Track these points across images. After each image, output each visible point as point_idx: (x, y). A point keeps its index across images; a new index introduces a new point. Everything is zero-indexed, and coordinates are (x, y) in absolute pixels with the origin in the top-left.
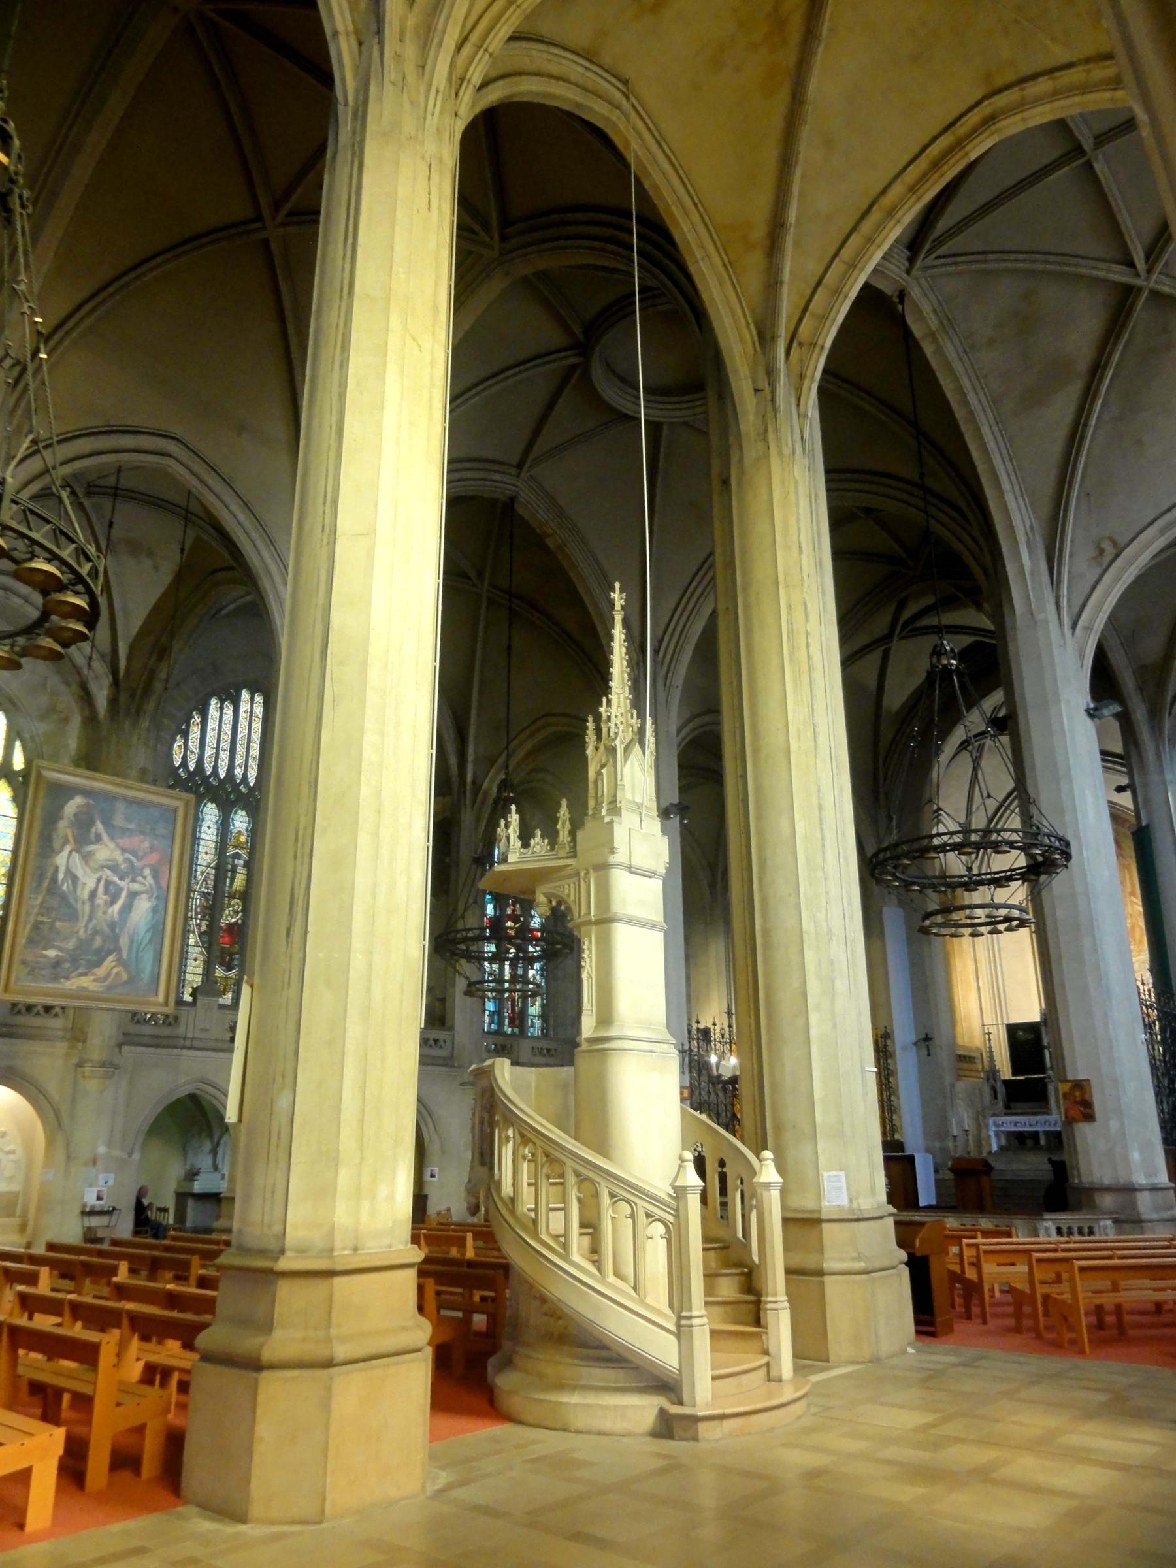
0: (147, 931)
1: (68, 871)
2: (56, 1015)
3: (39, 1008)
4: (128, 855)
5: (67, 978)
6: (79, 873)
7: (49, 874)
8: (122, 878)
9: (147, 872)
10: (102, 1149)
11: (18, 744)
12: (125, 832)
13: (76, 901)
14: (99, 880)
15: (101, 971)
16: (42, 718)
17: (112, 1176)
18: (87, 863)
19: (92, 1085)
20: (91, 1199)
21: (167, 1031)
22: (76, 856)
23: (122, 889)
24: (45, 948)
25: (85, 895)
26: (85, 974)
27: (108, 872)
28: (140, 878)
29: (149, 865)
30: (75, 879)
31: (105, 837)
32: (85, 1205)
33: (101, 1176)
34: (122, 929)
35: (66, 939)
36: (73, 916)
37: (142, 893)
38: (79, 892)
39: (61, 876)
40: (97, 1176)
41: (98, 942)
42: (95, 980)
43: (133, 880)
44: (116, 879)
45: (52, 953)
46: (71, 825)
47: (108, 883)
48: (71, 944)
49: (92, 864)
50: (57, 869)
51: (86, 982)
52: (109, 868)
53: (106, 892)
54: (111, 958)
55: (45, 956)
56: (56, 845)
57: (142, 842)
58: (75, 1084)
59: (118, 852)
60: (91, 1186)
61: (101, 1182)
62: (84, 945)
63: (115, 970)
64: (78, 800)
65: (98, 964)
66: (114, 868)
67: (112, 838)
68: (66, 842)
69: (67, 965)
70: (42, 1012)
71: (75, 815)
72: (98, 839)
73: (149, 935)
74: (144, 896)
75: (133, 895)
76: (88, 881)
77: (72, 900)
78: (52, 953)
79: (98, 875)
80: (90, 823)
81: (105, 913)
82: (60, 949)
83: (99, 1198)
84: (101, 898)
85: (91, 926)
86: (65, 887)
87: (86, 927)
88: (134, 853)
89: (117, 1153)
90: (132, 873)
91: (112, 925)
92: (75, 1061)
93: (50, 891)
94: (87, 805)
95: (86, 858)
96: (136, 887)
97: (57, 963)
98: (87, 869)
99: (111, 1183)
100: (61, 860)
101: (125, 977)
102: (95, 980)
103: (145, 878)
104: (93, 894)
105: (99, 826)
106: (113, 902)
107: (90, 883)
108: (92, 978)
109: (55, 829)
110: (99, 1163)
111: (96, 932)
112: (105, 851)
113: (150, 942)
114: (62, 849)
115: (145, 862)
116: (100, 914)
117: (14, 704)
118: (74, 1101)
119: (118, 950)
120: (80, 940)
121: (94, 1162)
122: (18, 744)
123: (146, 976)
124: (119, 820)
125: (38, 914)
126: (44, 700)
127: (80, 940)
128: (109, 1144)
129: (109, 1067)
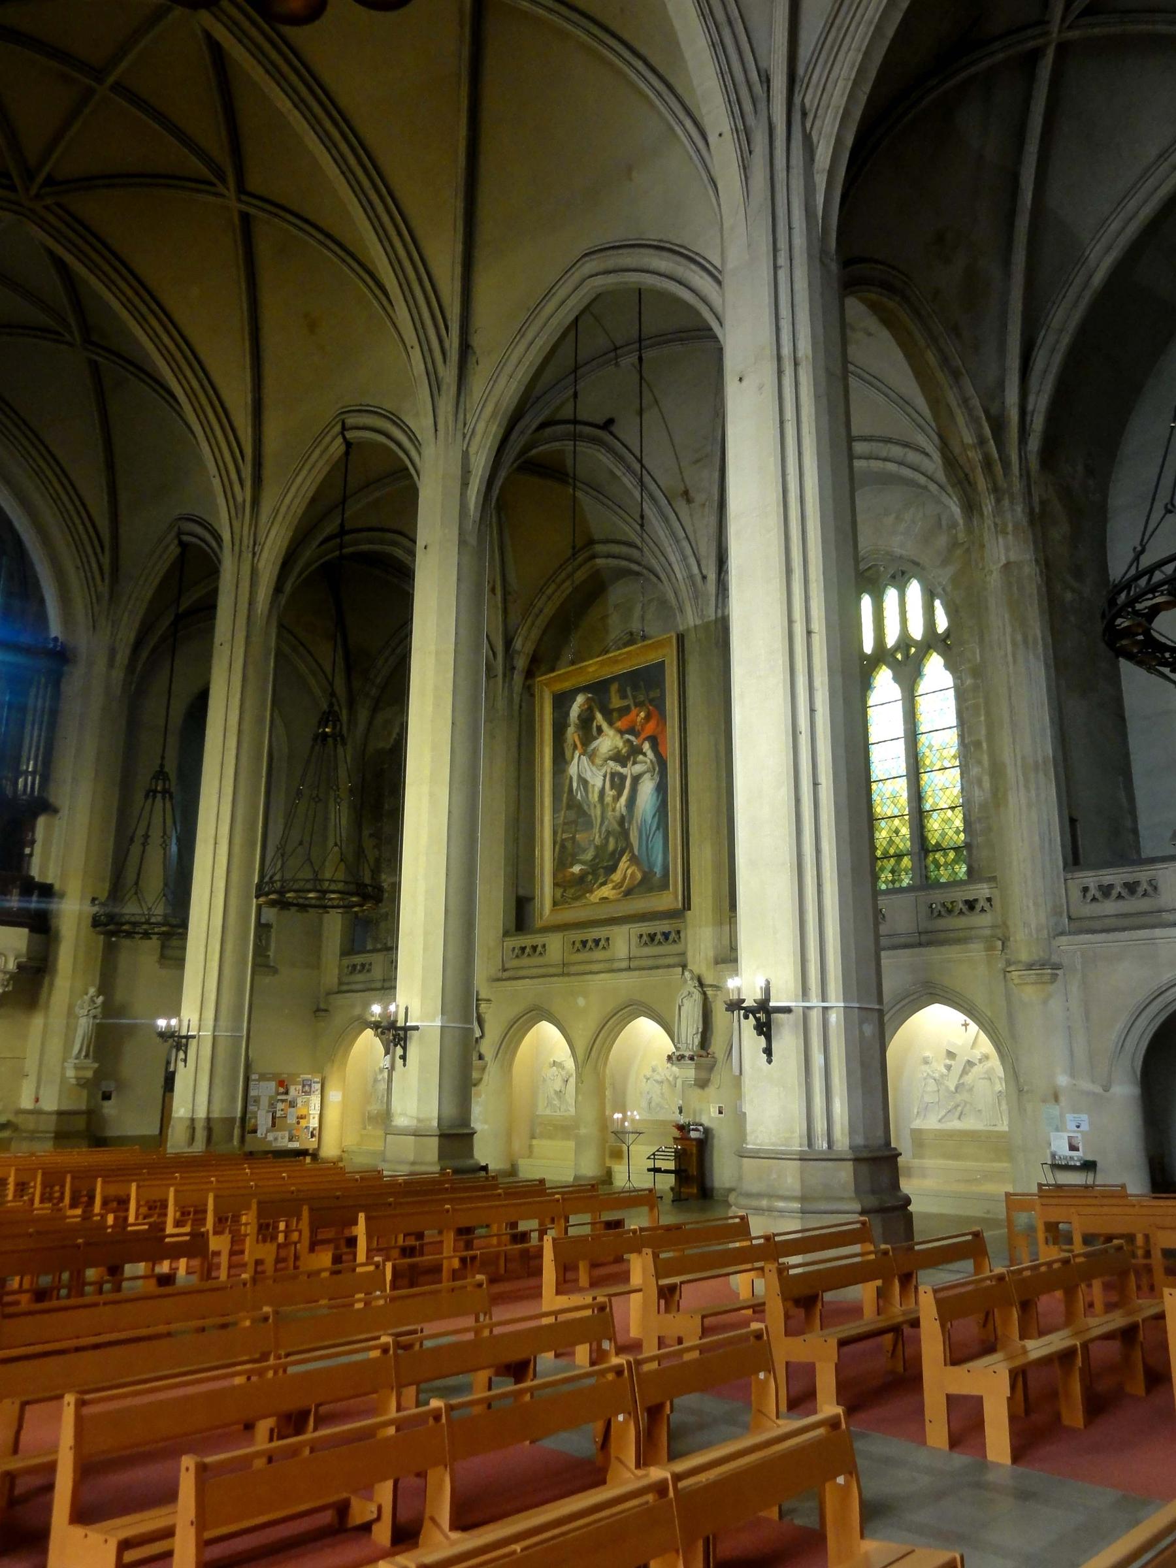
0: (654, 816)
1: (579, 776)
2: (983, 910)
3: (961, 905)
4: (627, 736)
5: (591, 892)
6: (588, 776)
7: (566, 789)
8: (624, 766)
9: (646, 747)
10: (1063, 1080)
11: (937, 603)
12: (625, 711)
14: (605, 776)
15: (617, 877)
16: (945, 562)
17: (1085, 1117)
18: (593, 763)
19: (1029, 993)
20: (1060, 1146)
21: (1143, 904)
22: (584, 758)
23: (626, 777)
24: (571, 866)
25: (594, 797)
26: (604, 884)
27: (611, 763)
28: (641, 757)
29: (646, 739)
30: (584, 782)
31: (605, 726)
32: (1053, 1156)
33: (1069, 1117)
34: (630, 823)
35: (584, 851)
36: (589, 825)
37: (645, 773)
38: (590, 795)
39: (575, 785)
40: (1062, 1116)
41: (611, 846)
42: (614, 888)
43: (635, 763)
44: (619, 769)
45: (576, 869)
46: (577, 726)
47: (613, 775)
48: (589, 855)
49: (598, 761)
50: (571, 778)
51: (606, 891)
52: (611, 759)
53: (612, 788)
54: (624, 859)
55: (573, 874)
56: (568, 754)
57: (638, 715)
58: (1008, 996)
59: (618, 737)
60: (1057, 1130)
61: (1071, 1126)
62: (600, 849)
63: (629, 871)
64: (580, 699)
65: (613, 869)
66: (619, 758)
67: (611, 724)
68: (575, 747)
69: (590, 877)
70: (965, 908)
71: (579, 716)
72: (600, 730)
74: (647, 776)
75: (636, 779)
76: (596, 780)
77: (586, 807)
78: (576, 869)
79: (603, 771)
80: (593, 718)
81: (614, 810)
82: (583, 863)
83: (1073, 1148)
84: (610, 793)
85: (604, 829)
86: (579, 797)
87: (600, 832)
88: (632, 731)
89: (1086, 1085)
90: (636, 751)
91: (622, 821)
92: (1001, 965)
93: (569, 807)
94: (588, 699)
95: (592, 757)
96: (638, 769)
97: (581, 879)
98: (594, 769)
99: (1085, 1127)
100: (573, 770)
101: (639, 876)
102: (614, 888)
103: (645, 755)
104: (602, 792)
105: (599, 716)
106: (620, 795)
107: (598, 783)
108: (610, 885)
110: (1062, 1099)
111: (609, 833)
112: (609, 741)
113: (658, 828)
114: (573, 758)
115: (643, 736)
116: (610, 814)
117: (917, 564)
118: (1011, 1016)
119: (629, 845)
120: (597, 847)
121: (1056, 1099)
122: (937, 603)
123: (658, 869)
124: (616, 702)
125: (563, 832)
126: (942, 541)
127: (597, 847)
128: (1072, 1075)
129: (1048, 968)
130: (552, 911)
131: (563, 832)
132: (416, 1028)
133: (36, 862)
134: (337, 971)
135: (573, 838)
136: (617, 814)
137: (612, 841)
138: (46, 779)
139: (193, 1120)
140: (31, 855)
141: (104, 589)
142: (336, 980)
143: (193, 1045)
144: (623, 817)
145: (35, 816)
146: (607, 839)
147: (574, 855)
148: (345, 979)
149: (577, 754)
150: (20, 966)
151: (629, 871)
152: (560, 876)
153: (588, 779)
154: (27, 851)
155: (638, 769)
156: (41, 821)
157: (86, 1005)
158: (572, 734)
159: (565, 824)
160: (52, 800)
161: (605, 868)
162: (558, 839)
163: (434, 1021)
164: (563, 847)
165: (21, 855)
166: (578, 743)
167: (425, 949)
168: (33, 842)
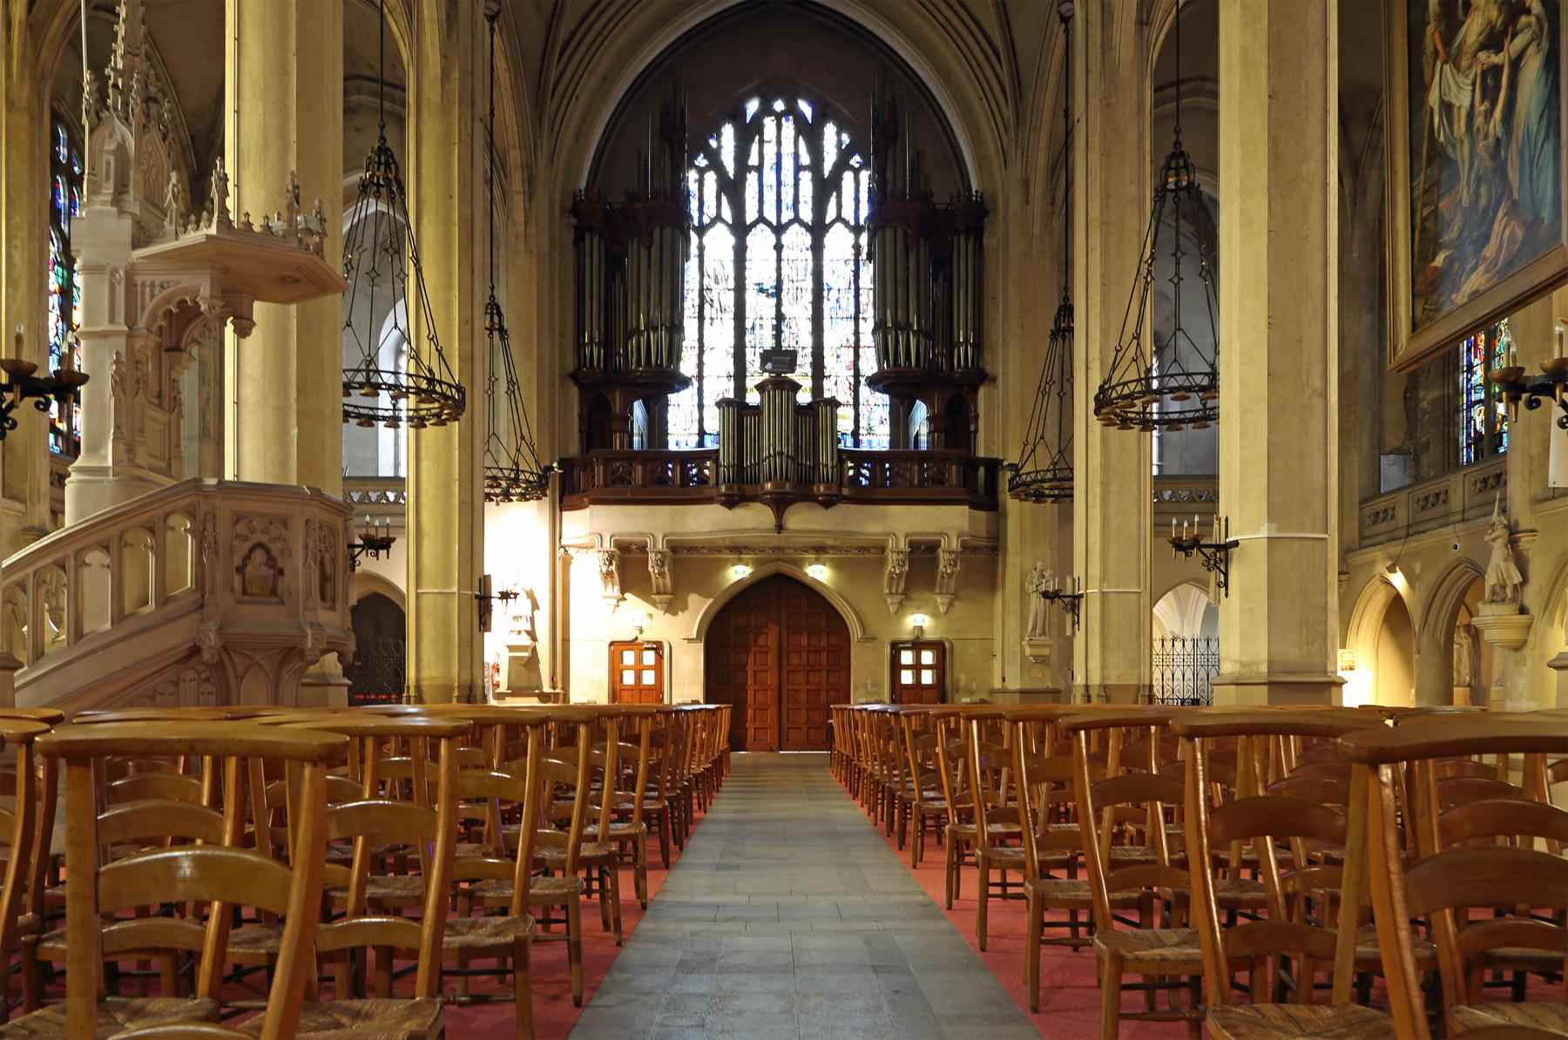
8: (1499, 49)
13: (1454, 147)
14: (1474, 84)
15: (1489, 251)
22: (1447, 67)
23: (1502, 67)
24: (1433, 259)
25: (1461, 126)
27: (1482, 56)
28: (1524, 19)
43: (1514, 36)
49: (1465, 63)
52: (1483, 47)
54: (1500, 214)
55: (1436, 268)
63: (1507, 233)
66: (1493, 41)
69: (1457, 265)
73: (1544, 122)
75: (1516, 64)
81: (1486, 137)
86: (1442, 139)
100: (1433, 99)
101: (1520, 234)
102: (1487, 271)
103: (1528, 12)
107: (1466, 102)
108: (1482, 268)
109: (1423, 53)
111: (1479, 179)
113: (1547, 137)
130: (1411, 340)
131: (1424, 206)
132: (1236, 544)
133: (981, 437)
134: (1356, 523)
135: (1435, 212)
136: (1491, 140)
137: (1483, 190)
138: (978, 347)
139: (1087, 687)
140: (976, 431)
141: (1009, 113)
142: (1356, 535)
143: (1083, 601)
144: (1498, 141)
145: (976, 391)
146: (1477, 194)
147: (1438, 236)
148: (1368, 532)
149: (1439, 63)
150: (964, 545)
151: (1507, 233)
152: (1420, 279)
153: (1454, 100)
154: (972, 428)
155: (1520, 42)
156: (982, 392)
157: (1035, 581)
158: (1432, 34)
159: (1426, 191)
160: (988, 369)
161: (1474, 242)
162: (1418, 221)
163: (1258, 531)
164: (1424, 230)
165: (969, 433)
166: (1440, 47)
167: (1242, 435)
168: (977, 417)
